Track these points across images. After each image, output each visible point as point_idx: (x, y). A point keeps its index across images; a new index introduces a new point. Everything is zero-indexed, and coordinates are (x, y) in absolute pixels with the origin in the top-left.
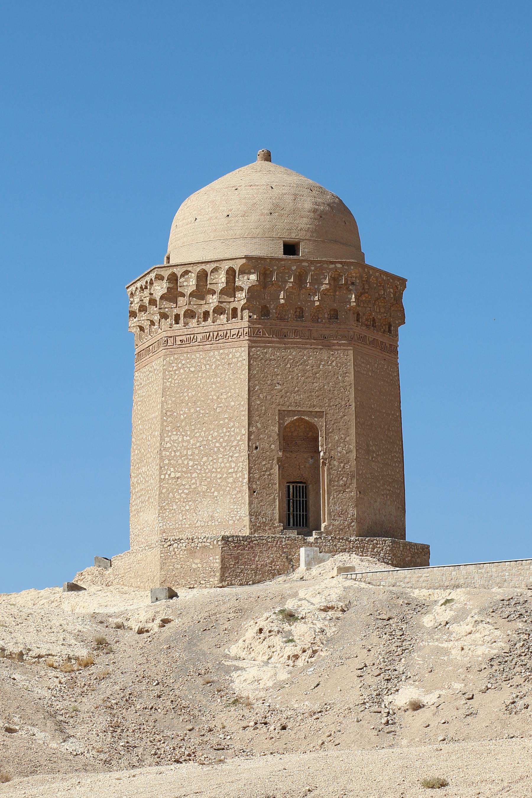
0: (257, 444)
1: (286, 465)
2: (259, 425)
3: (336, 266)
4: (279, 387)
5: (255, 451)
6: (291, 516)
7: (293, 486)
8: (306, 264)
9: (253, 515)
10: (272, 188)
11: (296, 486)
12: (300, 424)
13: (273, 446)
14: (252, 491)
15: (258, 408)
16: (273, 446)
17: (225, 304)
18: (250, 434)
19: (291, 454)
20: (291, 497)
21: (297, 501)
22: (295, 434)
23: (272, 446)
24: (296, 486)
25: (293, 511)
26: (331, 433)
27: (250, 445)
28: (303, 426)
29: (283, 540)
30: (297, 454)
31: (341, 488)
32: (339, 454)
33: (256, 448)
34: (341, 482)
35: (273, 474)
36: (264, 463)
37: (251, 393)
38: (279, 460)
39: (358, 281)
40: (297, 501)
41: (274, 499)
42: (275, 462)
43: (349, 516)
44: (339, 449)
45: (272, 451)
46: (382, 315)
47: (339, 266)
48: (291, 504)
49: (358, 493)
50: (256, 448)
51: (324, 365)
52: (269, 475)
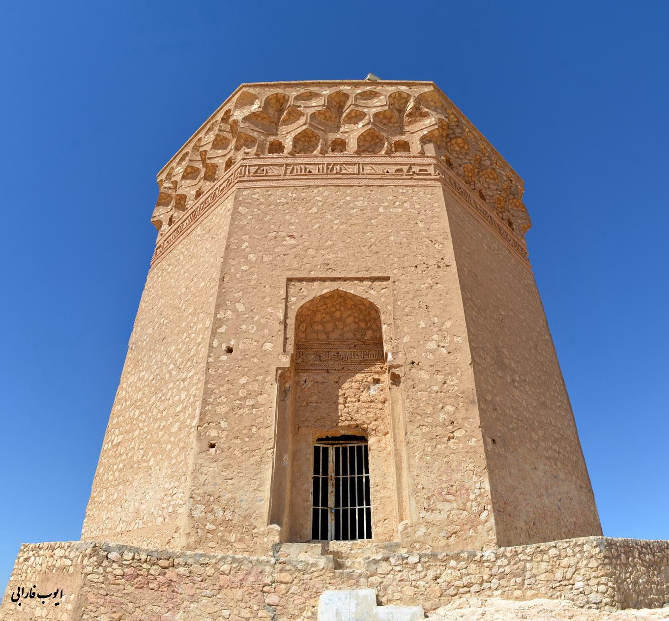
0: (232, 343)
1: (315, 398)
4: (293, 242)
5: (224, 358)
6: (331, 518)
7: (337, 450)
9: (199, 502)
11: (345, 449)
12: (345, 315)
14: (206, 445)
15: (241, 277)
16: (268, 346)
17: (217, 159)
18: (217, 323)
19: (325, 375)
21: (345, 480)
22: (334, 336)
24: (345, 449)
25: (337, 504)
27: (215, 344)
28: (350, 320)
29: (268, 569)
30: (340, 374)
31: (439, 431)
32: (431, 356)
33: (230, 350)
34: (442, 417)
35: (263, 405)
36: (243, 381)
37: (232, 254)
38: (282, 376)
40: (345, 480)
41: (269, 467)
42: (271, 378)
43: (472, 497)
44: (432, 345)
45: (266, 353)
48: (331, 489)
49: (489, 440)
51: (386, 208)
52: (253, 406)
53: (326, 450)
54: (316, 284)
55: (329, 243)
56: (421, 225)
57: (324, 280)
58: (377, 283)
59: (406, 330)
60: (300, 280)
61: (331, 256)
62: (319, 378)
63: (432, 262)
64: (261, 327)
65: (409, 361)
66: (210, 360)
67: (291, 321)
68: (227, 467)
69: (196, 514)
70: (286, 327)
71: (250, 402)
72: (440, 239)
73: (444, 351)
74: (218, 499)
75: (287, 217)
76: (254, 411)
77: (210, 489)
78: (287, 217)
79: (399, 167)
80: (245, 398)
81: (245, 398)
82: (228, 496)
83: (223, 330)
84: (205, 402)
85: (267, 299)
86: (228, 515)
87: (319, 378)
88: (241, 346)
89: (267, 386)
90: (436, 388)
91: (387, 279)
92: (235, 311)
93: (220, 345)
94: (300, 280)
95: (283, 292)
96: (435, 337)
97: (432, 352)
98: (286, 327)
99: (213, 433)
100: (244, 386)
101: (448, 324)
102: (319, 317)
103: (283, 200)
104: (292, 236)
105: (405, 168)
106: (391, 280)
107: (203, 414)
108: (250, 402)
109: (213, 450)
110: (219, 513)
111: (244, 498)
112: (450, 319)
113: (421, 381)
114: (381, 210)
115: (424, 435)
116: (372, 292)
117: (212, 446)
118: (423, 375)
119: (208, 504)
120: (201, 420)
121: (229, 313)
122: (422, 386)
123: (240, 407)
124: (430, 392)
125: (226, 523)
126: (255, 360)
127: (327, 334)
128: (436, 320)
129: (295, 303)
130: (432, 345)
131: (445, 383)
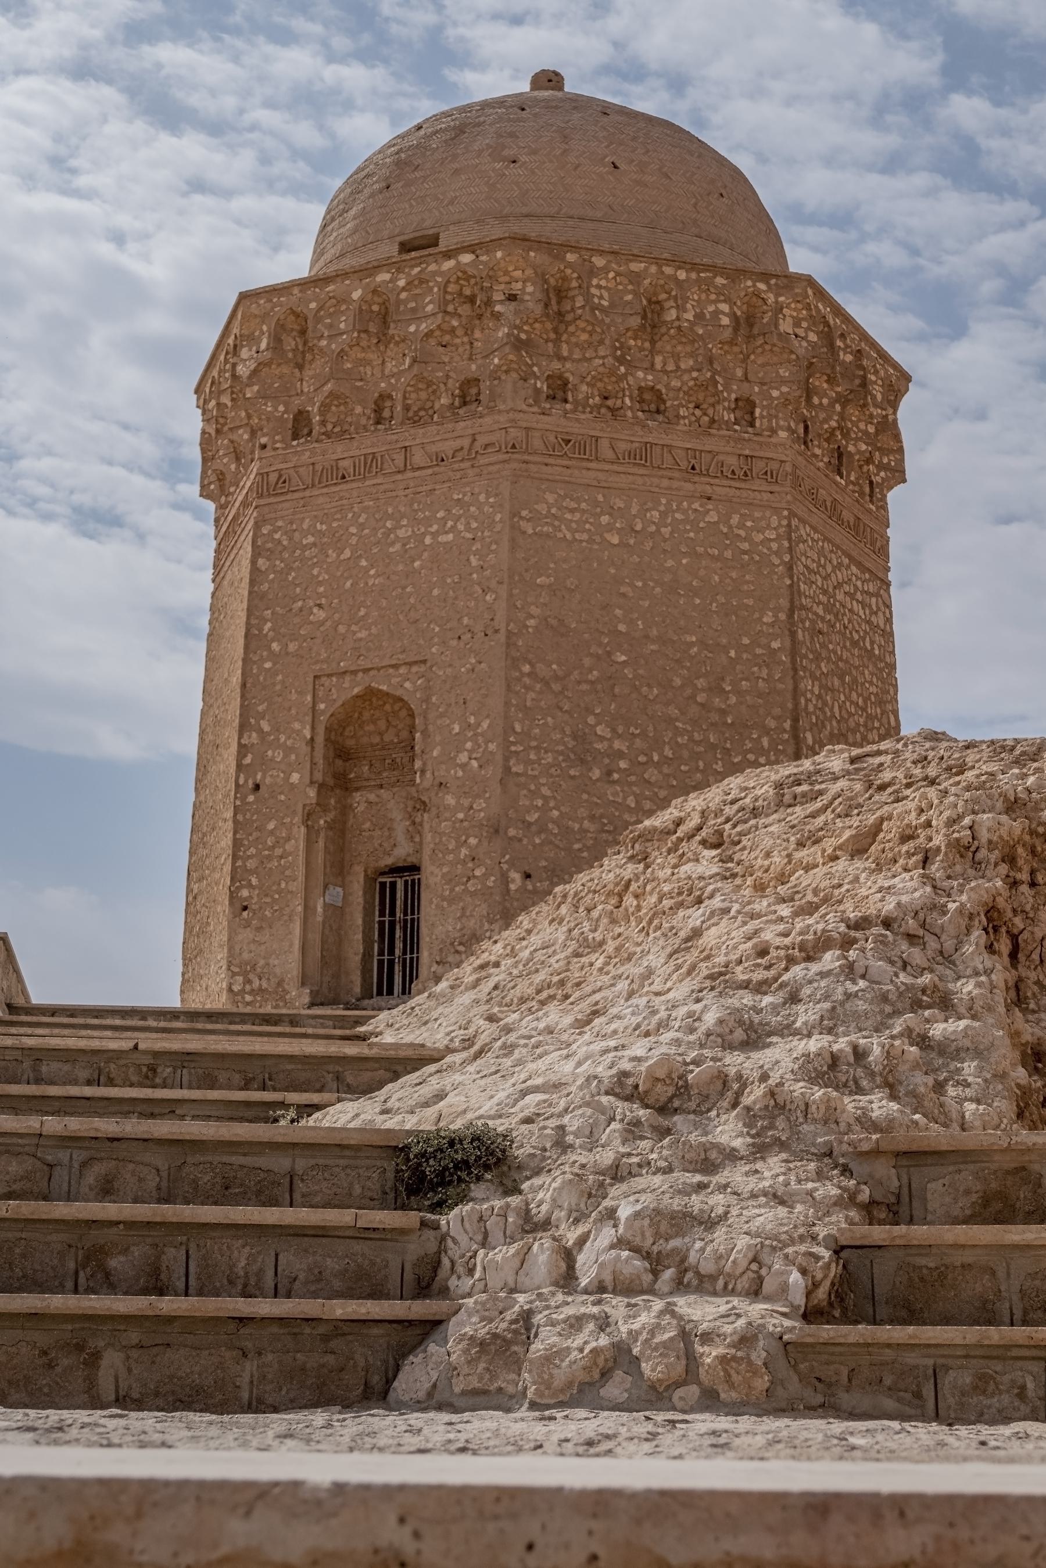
1: (367, 825)
2: (266, 726)
3: (458, 263)
4: (320, 614)
5: (251, 798)
8: (387, 276)
10: (616, 167)
13: (295, 777)
14: (238, 906)
20: (399, 914)
23: (296, 779)
24: (413, 881)
26: (442, 716)
27: (241, 781)
33: (257, 787)
34: (464, 851)
35: (290, 854)
36: (271, 826)
39: (530, 289)
44: (463, 758)
46: (686, 377)
47: (466, 258)
48: (398, 933)
50: (257, 787)
52: (281, 857)
53: (393, 885)
54: (348, 678)
55: (362, 613)
56: (474, 561)
57: (354, 673)
58: (415, 669)
59: (438, 738)
60: (330, 676)
61: (363, 634)
62: (372, 797)
63: (478, 628)
64: (288, 750)
65: (437, 782)
66: (238, 803)
67: (320, 739)
68: (259, 929)
69: (236, 988)
70: (313, 748)
71: (278, 851)
72: (493, 584)
73: (475, 764)
74: (254, 968)
75: (315, 572)
76: (282, 862)
77: (246, 956)
78: (315, 572)
79: (458, 443)
80: (273, 847)
81: (273, 847)
82: (262, 962)
83: (248, 760)
84: (235, 857)
85: (293, 712)
86: (265, 985)
87: (372, 797)
88: (268, 780)
89: (295, 830)
90: (461, 816)
91: (424, 662)
92: (260, 731)
93: (246, 781)
94: (330, 676)
95: (309, 698)
96: (469, 745)
97: (463, 766)
98: (313, 748)
99: (245, 893)
100: (272, 832)
101: (485, 725)
102: (366, 715)
103: (311, 539)
104: (320, 606)
105: (466, 442)
106: (428, 664)
107: (234, 869)
108: (278, 851)
109: (245, 913)
110: (256, 983)
111: (276, 962)
112: (488, 716)
113: (447, 808)
114: (428, 540)
115: (443, 875)
116: (407, 685)
117: (245, 908)
118: (450, 800)
119: (245, 974)
120: (232, 879)
121: (254, 735)
122: (447, 815)
123: (269, 858)
124: (454, 823)
125: (261, 990)
126: (283, 797)
127: (381, 734)
128: (472, 720)
129: (323, 712)
130: (463, 758)
131: (471, 808)
